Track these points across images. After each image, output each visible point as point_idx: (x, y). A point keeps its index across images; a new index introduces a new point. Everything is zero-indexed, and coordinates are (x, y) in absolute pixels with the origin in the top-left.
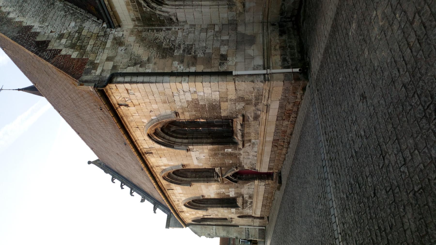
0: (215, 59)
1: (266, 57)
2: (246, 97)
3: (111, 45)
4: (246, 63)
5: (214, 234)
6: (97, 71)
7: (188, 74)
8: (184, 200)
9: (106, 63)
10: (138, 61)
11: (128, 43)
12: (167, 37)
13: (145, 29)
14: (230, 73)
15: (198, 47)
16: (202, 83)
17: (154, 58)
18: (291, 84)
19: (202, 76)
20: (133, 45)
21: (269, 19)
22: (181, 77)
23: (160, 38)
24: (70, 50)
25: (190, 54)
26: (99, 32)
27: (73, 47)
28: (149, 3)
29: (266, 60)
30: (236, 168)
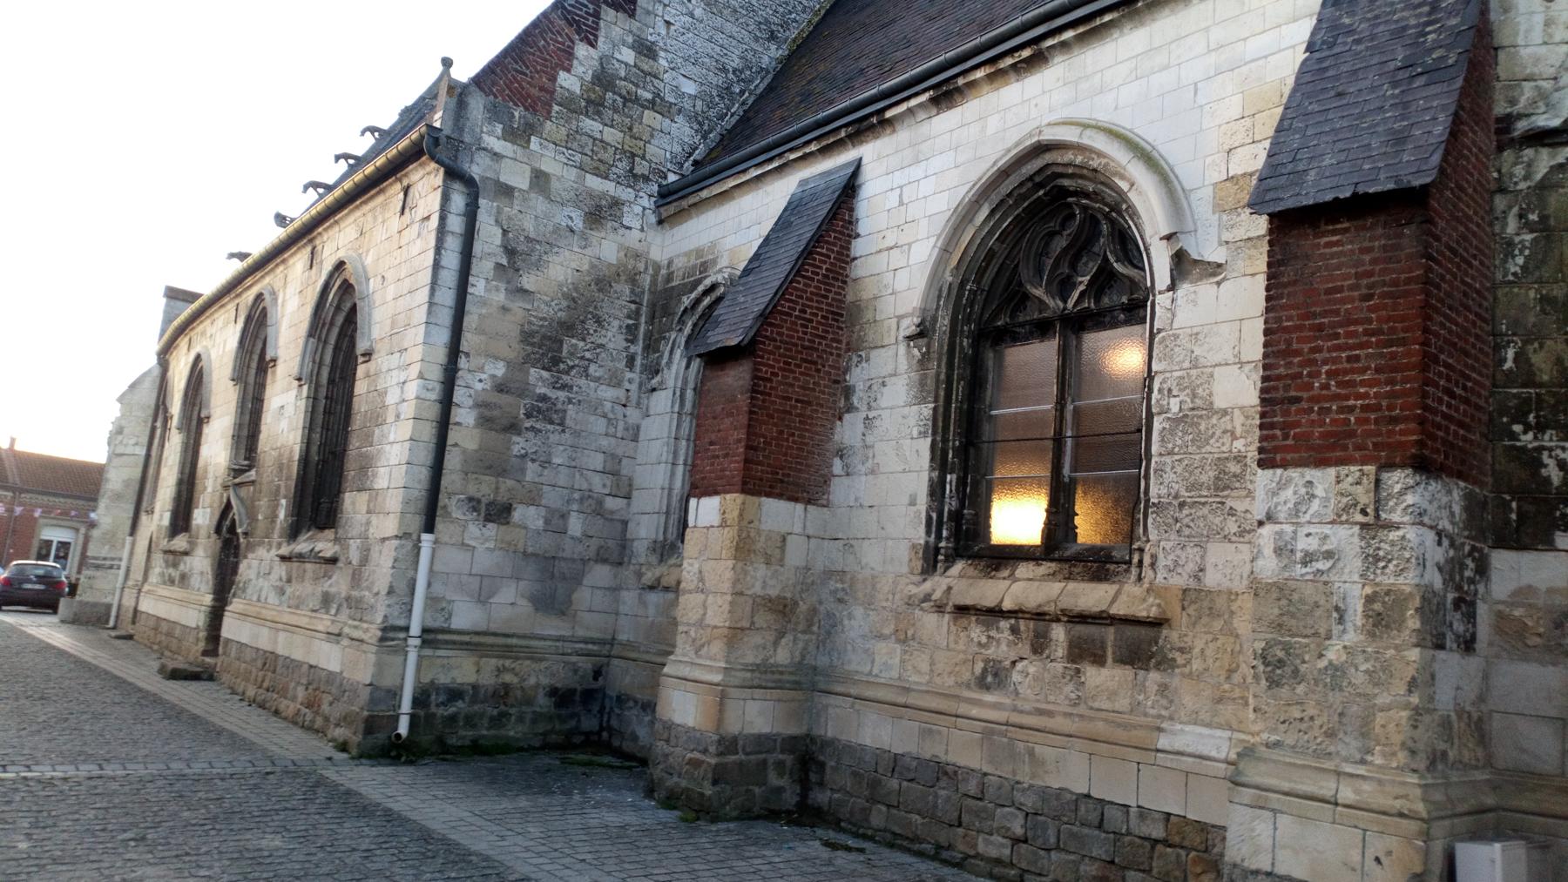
0: (497, 488)
1: (476, 639)
3: (593, 190)
4: (465, 579)
5: (120, 450)
7: (447, 403)
8: (209, 356)
9: (528, 169)
10: (524, 261)
12: (603, 355)
13: (643, 293)
14: (429, 527)
16: (411, 439)
17: (529, 307)
18: (362, 709)
19: (434, 441)
21: (622, 663)
23: (603, 332)
25: (528, 416)
29: (466, 638)
30: (246, 534)
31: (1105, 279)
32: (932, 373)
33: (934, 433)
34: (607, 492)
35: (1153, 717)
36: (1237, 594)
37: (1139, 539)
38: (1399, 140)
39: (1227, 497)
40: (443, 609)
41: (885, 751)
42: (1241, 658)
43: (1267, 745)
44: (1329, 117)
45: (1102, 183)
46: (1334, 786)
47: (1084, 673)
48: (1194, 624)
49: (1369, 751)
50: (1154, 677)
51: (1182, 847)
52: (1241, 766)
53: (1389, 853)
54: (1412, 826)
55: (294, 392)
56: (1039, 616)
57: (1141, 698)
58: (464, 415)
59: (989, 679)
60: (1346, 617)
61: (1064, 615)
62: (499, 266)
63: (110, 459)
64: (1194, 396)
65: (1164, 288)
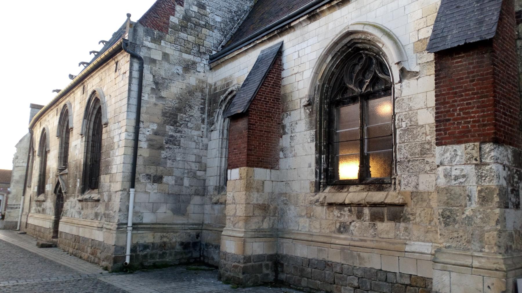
0: (157, 170)
1: (153, 226)
3: (185, 59)
4: (147, 204)
7: (136, 140)
9: (161, 52)
10: (161, 86)
12: (193, 119)
13: (206, 95)
14: (133, 186)
15: (176, 151)
16: (124, 154)
18: (112, 254)
20: (184, 82)
21: (206, 231)
22: (134, 132)
23: (192, 111)
25: (167, 143)
29: (149, 226)
31: (375, 80)
32: (314, 118)
33: (316, 140)
34: (197, 169)
35: (403, 239)
36: (431, 193)
37: (394, 175)
38: (480, 22)
39: (425, 157)
40: (139, 216)
41: (305, 258)
42: (434, 216)
43: (446, 247)
44: (454, 15)
45: (372, 45)
46: (471, 261)
47: (377, 225)
48: (416, 205)
49: (483, 247)
50: (402, 225)
51: (417, 287)
52: (436, 256)
53: (493, 284)
54: (501, 274)
55: (80, 140)
56: (359, 205)
57: (398, 233)
58: (143, 144)
59: (342, 229)
60: (472, 199)
61: (368, 204)
62: (152, 89)
63: (14, 168)
64: (411, 121)
65: (397, 82)
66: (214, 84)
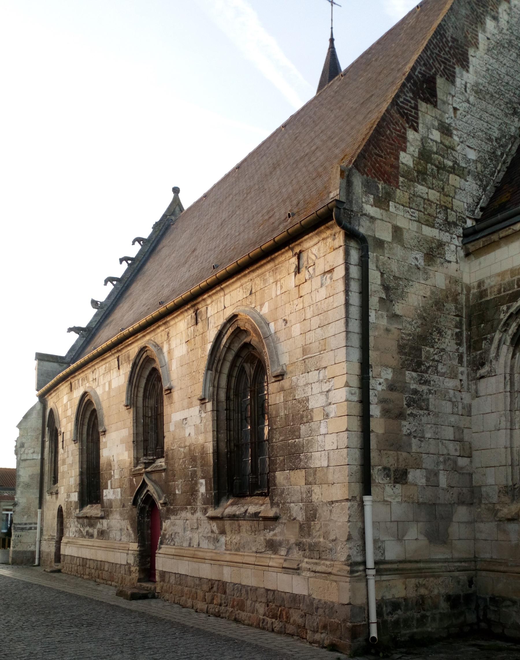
0: (398, 459)
1: (401, 566)
2: (316, 525)
6: (372, 206)
11: (431, 273)
12: (445, 356)
13: (462, 308)
14: (367, 491)
15: (423, 421)
16: (347, 430)
17: (400, 327)
18: (344, 621)
19: (360, 430)
20: (427, 283)
21: (484, 573)
22: (359, 386)
23: (443, 340)
24: (417, 150)
25: (409, 405)
26: (456, 212)
27: (422, 155)
28: (517, 318)
29: (395, 566)
34: (458, 454)
40: (379, 547)
58: (375, 410)
62: (381, 299)
66: (476, 284)
